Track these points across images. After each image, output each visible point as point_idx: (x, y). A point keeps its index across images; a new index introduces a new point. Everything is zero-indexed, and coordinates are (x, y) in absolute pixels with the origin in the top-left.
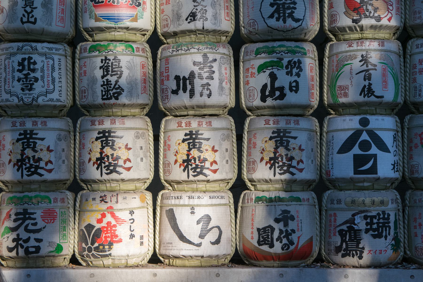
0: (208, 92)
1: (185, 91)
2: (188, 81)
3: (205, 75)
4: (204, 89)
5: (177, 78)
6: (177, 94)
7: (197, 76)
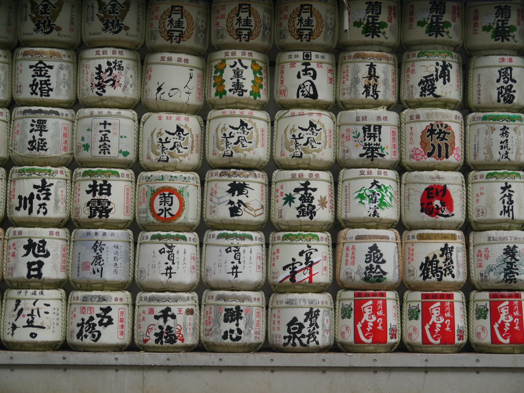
0: (44, 211)
1: (25, 208)
2: (28, 201)
3: (42, 197)
4: (41, 207)
5: (20, 197)
6: (19, 210)
7: (35, 197)
